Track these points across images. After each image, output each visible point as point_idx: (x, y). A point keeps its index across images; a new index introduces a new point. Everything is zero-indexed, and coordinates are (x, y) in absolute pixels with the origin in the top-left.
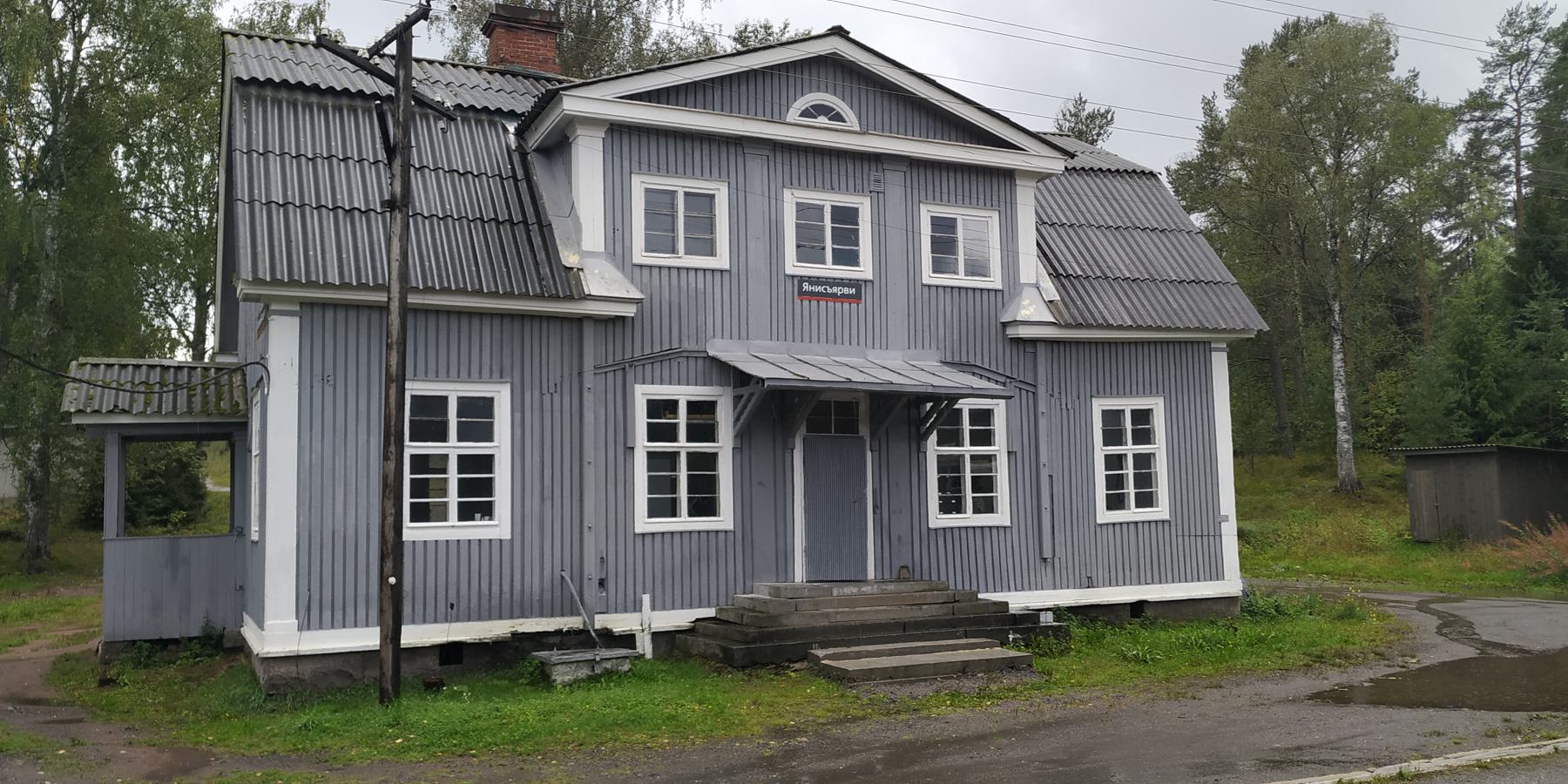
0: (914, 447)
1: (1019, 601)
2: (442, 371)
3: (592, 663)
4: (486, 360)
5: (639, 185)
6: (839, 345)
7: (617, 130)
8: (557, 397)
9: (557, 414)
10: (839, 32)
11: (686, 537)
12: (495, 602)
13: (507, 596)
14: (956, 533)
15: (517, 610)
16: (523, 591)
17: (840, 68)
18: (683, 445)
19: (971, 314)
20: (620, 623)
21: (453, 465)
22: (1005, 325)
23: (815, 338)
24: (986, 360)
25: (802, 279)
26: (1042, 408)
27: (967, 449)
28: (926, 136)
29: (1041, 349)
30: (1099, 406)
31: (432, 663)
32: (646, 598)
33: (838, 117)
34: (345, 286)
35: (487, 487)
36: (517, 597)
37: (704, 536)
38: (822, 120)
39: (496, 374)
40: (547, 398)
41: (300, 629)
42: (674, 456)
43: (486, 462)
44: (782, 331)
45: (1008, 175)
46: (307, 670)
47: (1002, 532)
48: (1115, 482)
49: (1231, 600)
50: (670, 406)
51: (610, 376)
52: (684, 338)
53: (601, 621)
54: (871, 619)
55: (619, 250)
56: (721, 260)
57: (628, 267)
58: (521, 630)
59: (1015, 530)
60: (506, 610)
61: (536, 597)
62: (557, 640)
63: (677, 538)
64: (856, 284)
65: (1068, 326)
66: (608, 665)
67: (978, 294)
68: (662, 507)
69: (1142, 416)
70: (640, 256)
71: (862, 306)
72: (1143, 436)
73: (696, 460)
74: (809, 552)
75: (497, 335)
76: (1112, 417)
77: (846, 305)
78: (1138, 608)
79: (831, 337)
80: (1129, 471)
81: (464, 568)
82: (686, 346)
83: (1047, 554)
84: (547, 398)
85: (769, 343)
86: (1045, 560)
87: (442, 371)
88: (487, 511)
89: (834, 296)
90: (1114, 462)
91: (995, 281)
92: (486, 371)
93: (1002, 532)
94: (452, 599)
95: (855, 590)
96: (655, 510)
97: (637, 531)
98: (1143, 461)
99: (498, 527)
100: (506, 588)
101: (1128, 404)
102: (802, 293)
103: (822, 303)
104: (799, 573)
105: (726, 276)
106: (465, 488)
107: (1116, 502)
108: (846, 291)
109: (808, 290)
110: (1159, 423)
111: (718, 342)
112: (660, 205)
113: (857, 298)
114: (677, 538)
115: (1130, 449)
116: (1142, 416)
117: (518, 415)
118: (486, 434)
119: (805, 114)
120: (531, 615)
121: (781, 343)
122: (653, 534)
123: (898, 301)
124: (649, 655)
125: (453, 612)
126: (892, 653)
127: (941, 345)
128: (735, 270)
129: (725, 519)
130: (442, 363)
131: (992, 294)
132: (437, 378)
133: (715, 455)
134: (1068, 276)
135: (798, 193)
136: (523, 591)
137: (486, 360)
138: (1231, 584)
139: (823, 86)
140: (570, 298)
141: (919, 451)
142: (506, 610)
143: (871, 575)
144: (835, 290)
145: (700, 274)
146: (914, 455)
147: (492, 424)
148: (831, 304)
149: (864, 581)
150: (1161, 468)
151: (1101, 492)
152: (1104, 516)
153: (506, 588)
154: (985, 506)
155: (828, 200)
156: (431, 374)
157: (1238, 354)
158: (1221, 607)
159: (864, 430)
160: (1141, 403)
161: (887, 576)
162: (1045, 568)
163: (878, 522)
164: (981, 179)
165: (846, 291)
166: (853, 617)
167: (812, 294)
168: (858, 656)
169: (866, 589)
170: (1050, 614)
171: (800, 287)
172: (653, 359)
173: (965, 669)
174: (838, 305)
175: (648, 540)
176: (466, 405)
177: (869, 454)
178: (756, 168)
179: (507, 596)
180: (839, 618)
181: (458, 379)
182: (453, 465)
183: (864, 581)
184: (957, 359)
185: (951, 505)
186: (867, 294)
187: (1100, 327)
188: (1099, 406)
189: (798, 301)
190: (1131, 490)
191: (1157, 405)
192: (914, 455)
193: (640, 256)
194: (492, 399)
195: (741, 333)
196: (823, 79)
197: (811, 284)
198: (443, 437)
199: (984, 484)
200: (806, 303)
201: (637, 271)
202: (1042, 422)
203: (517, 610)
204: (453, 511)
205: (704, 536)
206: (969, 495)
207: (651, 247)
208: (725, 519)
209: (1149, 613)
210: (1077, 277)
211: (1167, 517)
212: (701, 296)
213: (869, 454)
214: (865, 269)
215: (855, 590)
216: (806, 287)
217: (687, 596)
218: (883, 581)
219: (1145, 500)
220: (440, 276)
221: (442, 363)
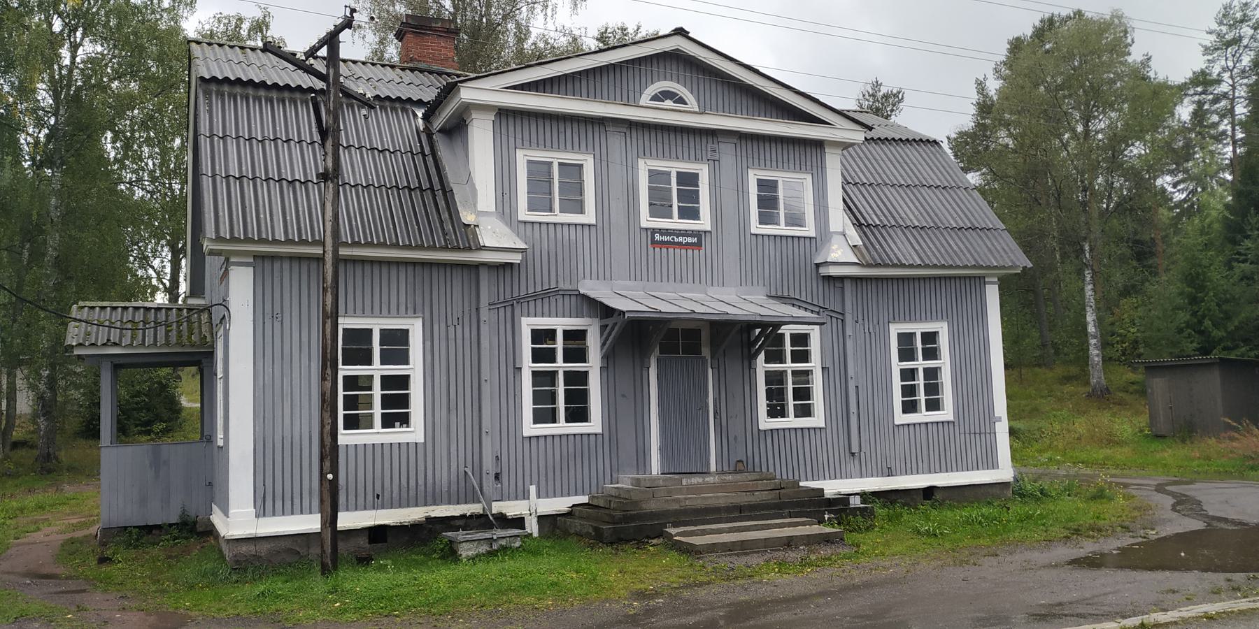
0: (746, 364)
1: (832, 488)
2: (368, 308)
3: (490, 541)
4: (402, 299)
5: (522, 158)
6: (685, 284)
7: (504, 114)
8: (459, 328)
9: (459, 342)
10: (681, 32)
11: (564, 439)
12: (412, 493)
13: (421, 488)
14: (781, 433)
15: (429, 499)
16: (434, 483)
17: (682, 61)
18: (560, 365)
19: (791, 257)
20: (512, 508)
21: (377, 383)
22: (818, 265)
23: (665, 278)
24: (803, 294)
25: (654, 231)
26: (849, 332)
27: (789, 366)
28: (751, 114)
29: (848, 285)
30: (895, 329)
31: (363, 542)
32: (533, 489)
33: (681, 101)
34: (289, 242)
35: (404, 401)
36: (430, 489)
37: (578, 438)
38: (668, 103)
39: (410, 311)
40: (451, 329)
41: (257, 516)
42: (554, 374)
43: (403, 381)
44: (638, 273)
45: (819, 145)
46: (264, 548)
47: (818, 432)
48: (909, 391)
49: (1004, 485)
50: (550, 334)
51: (502, 311)
52: (560, 280)
53: (497, 507)
55: (507, 210)
56: (589, 217)
57: (515, 224)
58: (433, 515)
59: (829, 431)
60: (421, 499)
61: (445, 489)
62: (461, 523)
63: (557, 440)
65: (869, 266)
66: (503, 542)
67: (796, 240)
68: (545, 415)
69: (930, 338)
70: (524, 214)
71: (702, 252)
72: (931, 354)
73: (569, 376)
74: (662, 449)
75: (411, 279)
76: (906, 339)
77: (690, 251)
78: (929, 492)
79: (678, 278)
80: (920, 381)
81: (387, 465)
82: (561, 286)
83: (855, 449)
84: (451, 329)
85: (628, 283)
86: (853, 454)
87: (368, 308)
88: (405, 420)
89: (680, 244)
90: (908, 374)
91: (809, 230)
92: (402, 308)
93: (818, 432)
94: (378, 490)
95: (700, 480)
96: (539, 417)
97: (525, 434)
98: (932, 374)
99: (414, 433)
100: (421, 482)
101: (918, 328)
102: (654, 242)
103: (671, 250)
104: (655, 467)
105: (593, 229)
106: (387, 402)
107: (910, 407)
108: (690, 240)
109: (660, 240)
110: (944, 343)
111: (588, 282)
112: (540, 174)
113: (698, 245)
114: (557, 440)
115: (920, 364)
116: (930, 338)
117: (428, 343)
118: (403, 358)
119: (655, 98)
120: (441, 503)
121: (638, 283)
122: (538, 437)
124: (536, 534)
125: (379, 501)
126: (731, 530)
127: (767, 283)
128: (600, 225)
129: (595, 424)
130: (368, 302)
131: (807, 241)
132: (363, 314)
133: (586, 373)
134: (868, 225)
135: (649, 162)
136: (434, 483)
137: (402, 299)
138: (1004, 472)
139: (668, 75)
140: (469, 249)
141: (750, 367)
142: (421, 499)
143: (713, 468)
144: (680, 239)
145: (572, 228)
146: (747, 371)
147: (407, 350)
148: (677, 251)
149: (708, 473)
150: (946, 379)
151: (898, 399)
152: (900, 418)
153: (421, 482)
154: (805, 411)
155: (674, 167)
156: (359, 311)
157: (1006, 286)
158: (996, 491)
159: (706, 352)
160: (929, 327)
161: (726, 469)
162: (853, 460)
165: (690, 240)
166: (699, 502)
167: (663, 243)
168: (704, 533)
169: (709, 479)
170: (858, 498)
171: (653, 238)
172: (535, 297)
173: (789, 543)
174: (683, 251)
175: (534, 442)
176: (387, 336)
177: (710, 371)
178: (616, 142)
179: (421, 488)
181: (381, 315)
182: (377, 383)
183: (708, 473)
184: (779, 294)
185: (776, 411)
186: (706, 242)
187: (894, 266)
188: (895, 329)
189: (651, 249)
190: (922, 397)
191: (942, 328)
192: (747, 371)
193: (524, 214)
194: (407, 331)
195: (606, 275)
196: (668, 71)
197: (662, 234)
198: (370, 362)
199: (803, 394)
200: (657, 250)
201: (522, 226)
202: (849, 344)
203: (429, 499)
204: (378, 420)
205: (578, 438)
206: (791, 403)
207: (532, 207)
208: (595, 424)
209: (938, 496)
210: (876, 226)
211: (951, 418)
212: (573, 247)
213: (710, 371)
214: (704, 223)
215: (700, 480)
216: (657, 237)
217: (565, 487)
218: (723, 473)
219: (934, 405)
220: (364, 232)
221: (368, 302)
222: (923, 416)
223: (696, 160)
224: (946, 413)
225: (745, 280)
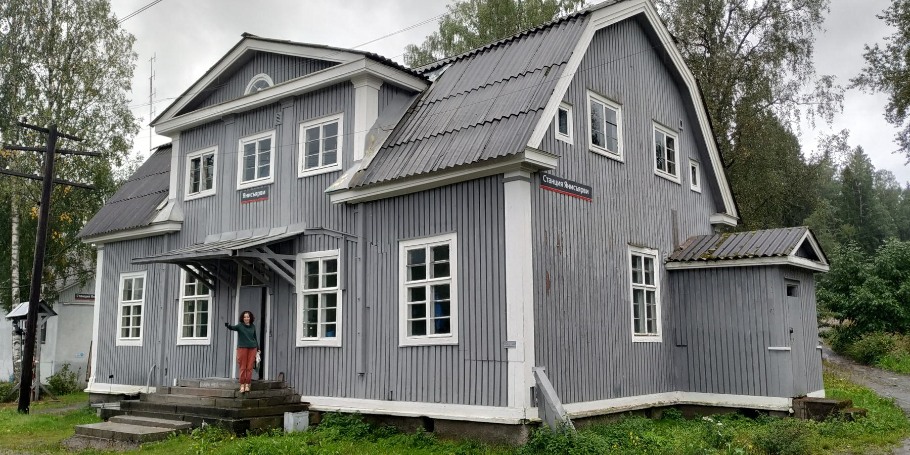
30: (405, 247)
45: (345, 85)
48: (418, 311)
49: (513, 428)
59: (344, 350)
64: (265, 187)
69: (441, 252)
72: (442, 270)
78: (428, 423)
80: (429, 300)
90: (418, 293)
96: (189, 332)
98: (442, 291)
101: (428, 243)
123: (286, 194)
138: (516, 409)
163: (272, 341)
164: (334, 92)
188: (405, 247)
190: (429, 318)
209: (438, 428)
216: (245, 196)
219: (443, 327)
222: (431, 338)
223: (266, 129)
225: (295, 219)
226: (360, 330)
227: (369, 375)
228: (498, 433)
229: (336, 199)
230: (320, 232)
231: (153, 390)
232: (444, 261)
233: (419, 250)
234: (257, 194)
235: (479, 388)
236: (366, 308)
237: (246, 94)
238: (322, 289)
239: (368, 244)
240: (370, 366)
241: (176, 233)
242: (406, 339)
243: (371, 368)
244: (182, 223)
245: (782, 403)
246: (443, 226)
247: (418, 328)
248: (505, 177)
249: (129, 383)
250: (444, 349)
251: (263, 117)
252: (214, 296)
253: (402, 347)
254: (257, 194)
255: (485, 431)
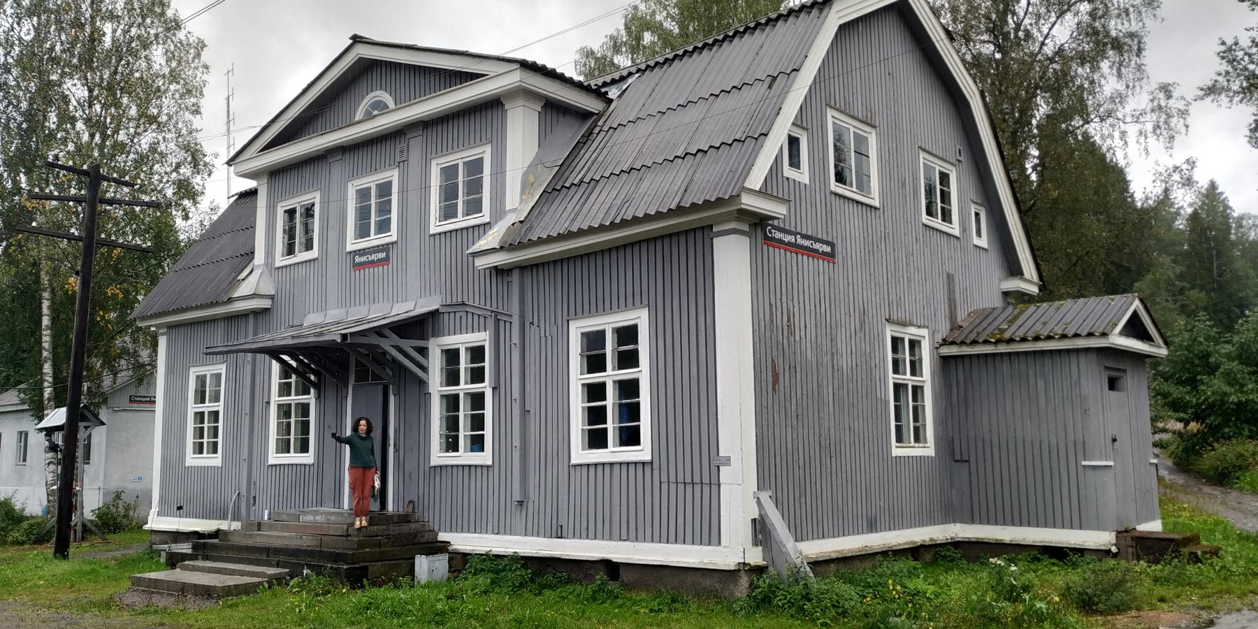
30: (577, 329)
45: (494, 104)
48: (596, 415)
49: (729, 576)
54: (277, 543)
64: (385, 248)
69: (628, 335)
72: (629, 359)
78: (612, 568)
90: (595, 392)
96: (284, 447)
98: (629, 389)
101: (608, 323)
113: (386, 261)
138: (732, 549)
143: (390, 507)
152: (580, 454)
158: (707, 582)
160: (623, 319)
162: (520, 512)
163: (397, 458)
164: (478, 115)
180: (258, 539)
188: (577, 329)
190: (611, 425)
195: (323, 308)
197: (360, 256)
216: (358, 259)
219: (630, 437)
222: (614, 452)
223: (385, 168)
224: (642, 452)
225: (426, 291)
226: (517, 443)
227: (531, 503)
228: (707, 582)
229: (483, 262)
230: (461, 308)
231: (236, 525)
232: (631, 347)
233: (598, 332)
234: (374, 257)
235: (680, 521)
236: (525, 412)
237: (357, 119)
238: (464, 387)
239: (527, 325)
240: (532, 491)
241: (265, 311)
242: (580, 454)
243: (533, 493)
244: (272, 297)
245: (1101, 539)
246: (630, 299)
247: (597, 439)
248: (715, 230)
249: (205, 516)
250: (632, 468)
251: (379, 152)
252: (318, 397)
253: (575, 466)
254: (374, 257)
255: (689, 579)
